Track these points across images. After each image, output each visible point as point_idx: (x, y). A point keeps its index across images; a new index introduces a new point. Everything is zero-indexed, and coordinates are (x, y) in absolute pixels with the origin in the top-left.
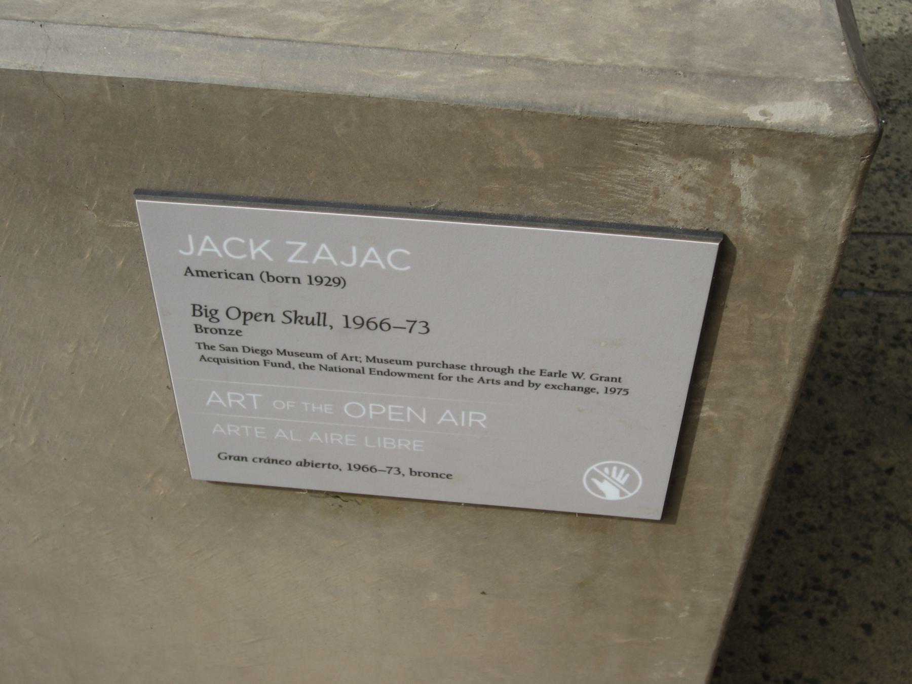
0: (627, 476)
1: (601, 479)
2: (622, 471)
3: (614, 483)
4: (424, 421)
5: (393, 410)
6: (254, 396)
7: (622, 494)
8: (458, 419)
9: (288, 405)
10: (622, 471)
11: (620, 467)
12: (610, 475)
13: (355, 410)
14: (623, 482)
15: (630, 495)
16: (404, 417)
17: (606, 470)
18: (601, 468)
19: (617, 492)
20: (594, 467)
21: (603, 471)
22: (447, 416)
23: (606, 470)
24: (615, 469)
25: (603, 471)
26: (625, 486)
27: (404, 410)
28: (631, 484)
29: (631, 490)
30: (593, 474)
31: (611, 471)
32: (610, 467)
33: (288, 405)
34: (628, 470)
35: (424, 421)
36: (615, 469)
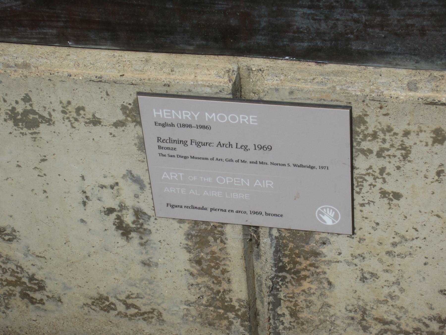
0: (334, 213)
1: (323, 214)
2: (331, 210)
3: (329, 216)
4: (248, 185)
5: (236, 180)
6: (181, 174)
7: (333, 222)
8: (262, 184)
9: (195, 178)
10: (331, 210)
11: (330, 208)
12: (327, 213)
13: (221, 180)
14: (332, 216)
15: (337, 222)
16: (240, 183)
17: (325, 210)
18: (322, 209)
19: (331, 221)
20: (319, 209)
21: (323, 210)
22: (257, 183)
23: (325, 210)
24: (328, 209)
25: (323, 210)
26: (334, 217)
27: (240, 180)
28: (336, 217)
29: (337, 220)
30: (320, 212)
31: (327, 211)
32: (326, 208)
33: (195, 178)
34: (334, 210)
35: (248, 185)
36: (328, 209)
